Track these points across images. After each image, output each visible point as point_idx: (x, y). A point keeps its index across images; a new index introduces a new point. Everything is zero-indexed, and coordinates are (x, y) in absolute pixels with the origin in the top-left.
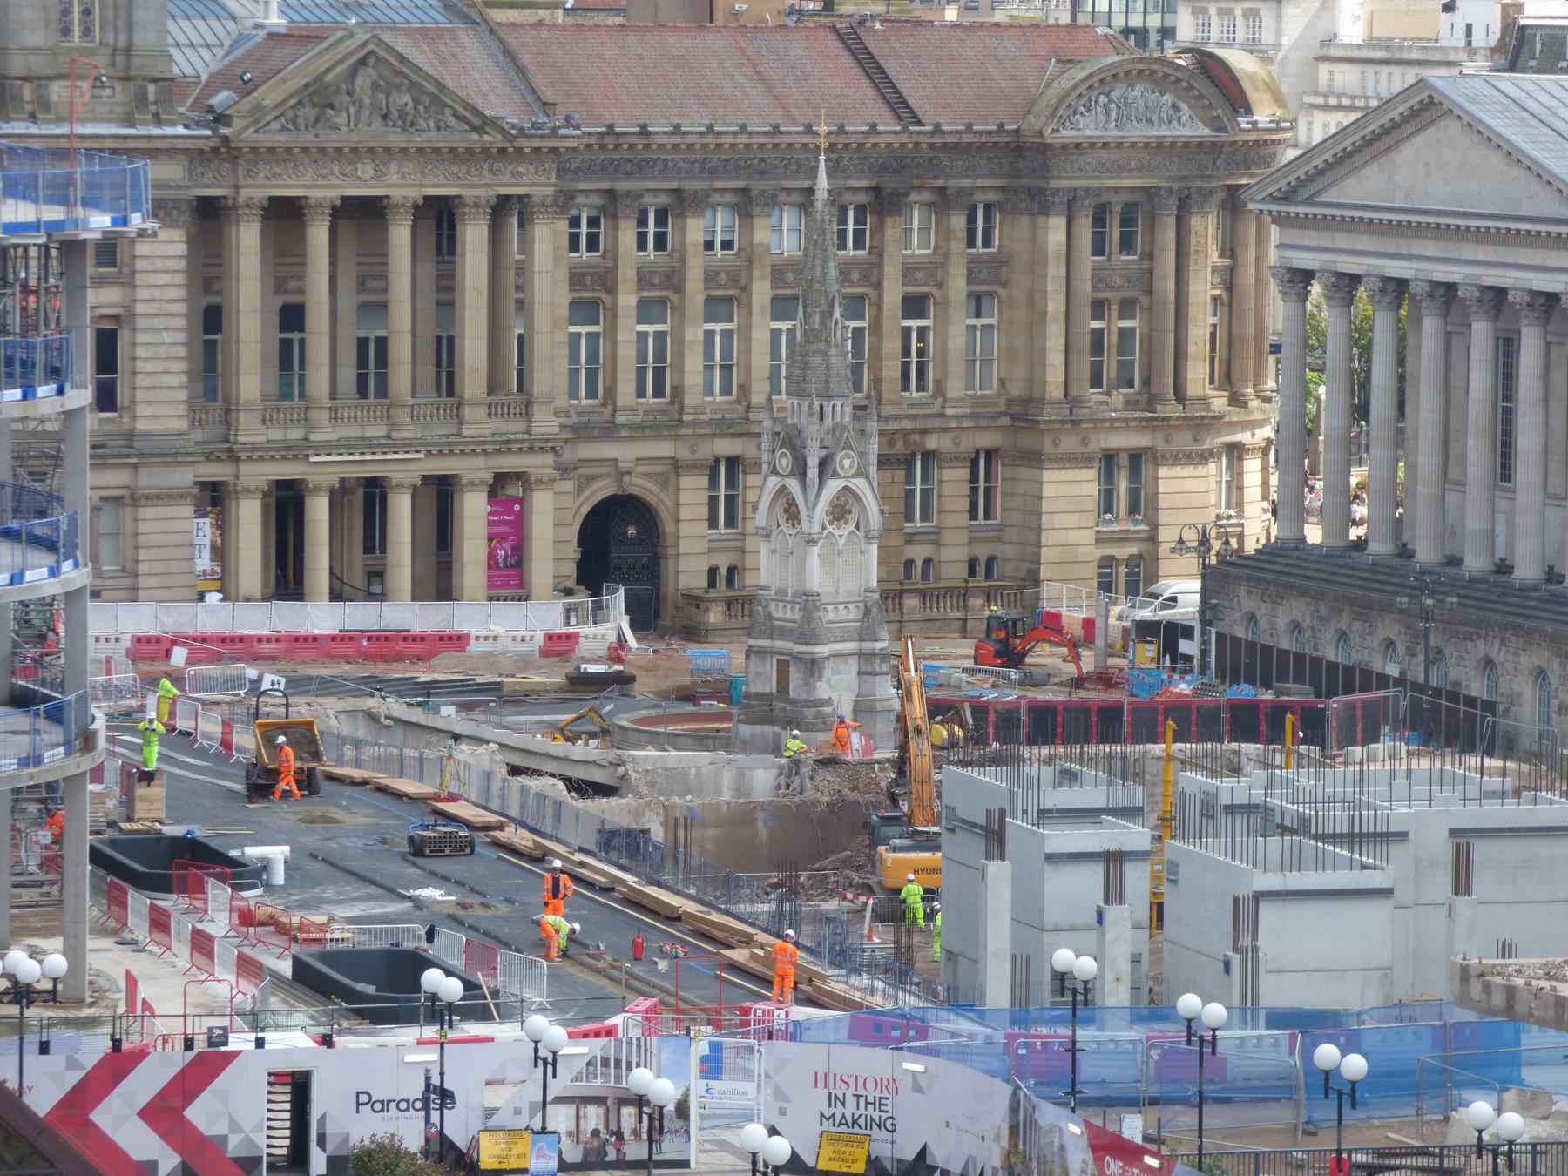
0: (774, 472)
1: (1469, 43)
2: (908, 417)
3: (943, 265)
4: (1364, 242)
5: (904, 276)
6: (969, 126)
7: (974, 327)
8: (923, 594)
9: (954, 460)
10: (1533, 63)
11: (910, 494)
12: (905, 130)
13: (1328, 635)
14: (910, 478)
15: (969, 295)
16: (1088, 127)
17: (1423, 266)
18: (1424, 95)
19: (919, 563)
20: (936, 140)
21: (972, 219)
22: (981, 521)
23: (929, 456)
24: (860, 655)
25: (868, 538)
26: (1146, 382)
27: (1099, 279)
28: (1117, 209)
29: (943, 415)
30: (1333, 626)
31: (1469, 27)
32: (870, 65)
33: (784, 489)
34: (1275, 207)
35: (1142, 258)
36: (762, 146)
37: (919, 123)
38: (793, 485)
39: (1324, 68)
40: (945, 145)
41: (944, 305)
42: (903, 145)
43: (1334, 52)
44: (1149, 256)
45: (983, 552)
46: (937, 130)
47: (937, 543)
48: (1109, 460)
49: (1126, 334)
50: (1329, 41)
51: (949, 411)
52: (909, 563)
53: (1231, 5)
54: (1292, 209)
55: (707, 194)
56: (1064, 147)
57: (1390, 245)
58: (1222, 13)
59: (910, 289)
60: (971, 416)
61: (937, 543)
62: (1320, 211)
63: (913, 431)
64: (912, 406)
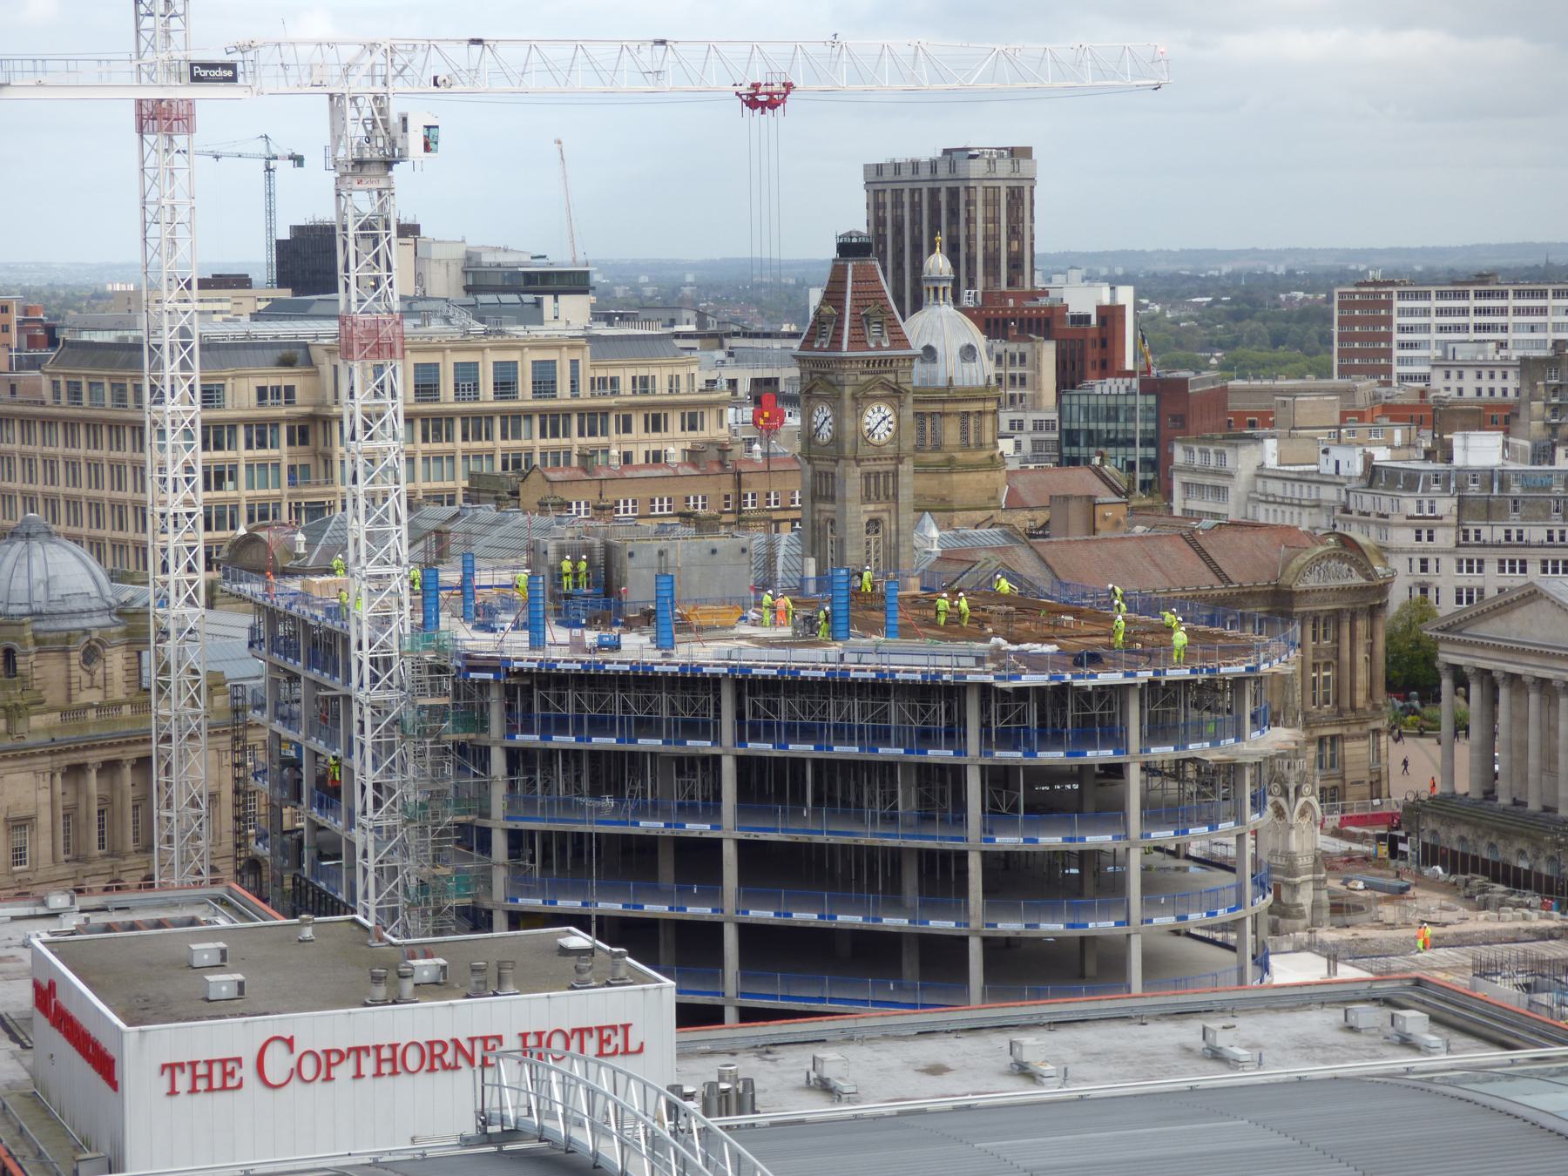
0: (1270, 794)
4: (1492, 654)
13: (1483, 845)
16: (1311, 582)
17: (1529, 669)
18: (1532, 589)
24: (1314, 880)
26: (1337, 701)
27: (1316, 651)
28: (1322, 620)
30: (1486, 840)
31: (1337, 463)
33: (1276, 802)
34: (1440, 635)
37: (1231, 583)
38: (1282, 801)
39: (1260, 482)
43: (1265, 473)
44: (1338, 641)
46: (1241, 586)
48: (1321, 740)
49: (1326, 679)
50: (1261, 466)
54: (1451, 636)
56: (1301, 592)
57: (1509, 657)
58: (1201, 451)
62: (1468, 639)
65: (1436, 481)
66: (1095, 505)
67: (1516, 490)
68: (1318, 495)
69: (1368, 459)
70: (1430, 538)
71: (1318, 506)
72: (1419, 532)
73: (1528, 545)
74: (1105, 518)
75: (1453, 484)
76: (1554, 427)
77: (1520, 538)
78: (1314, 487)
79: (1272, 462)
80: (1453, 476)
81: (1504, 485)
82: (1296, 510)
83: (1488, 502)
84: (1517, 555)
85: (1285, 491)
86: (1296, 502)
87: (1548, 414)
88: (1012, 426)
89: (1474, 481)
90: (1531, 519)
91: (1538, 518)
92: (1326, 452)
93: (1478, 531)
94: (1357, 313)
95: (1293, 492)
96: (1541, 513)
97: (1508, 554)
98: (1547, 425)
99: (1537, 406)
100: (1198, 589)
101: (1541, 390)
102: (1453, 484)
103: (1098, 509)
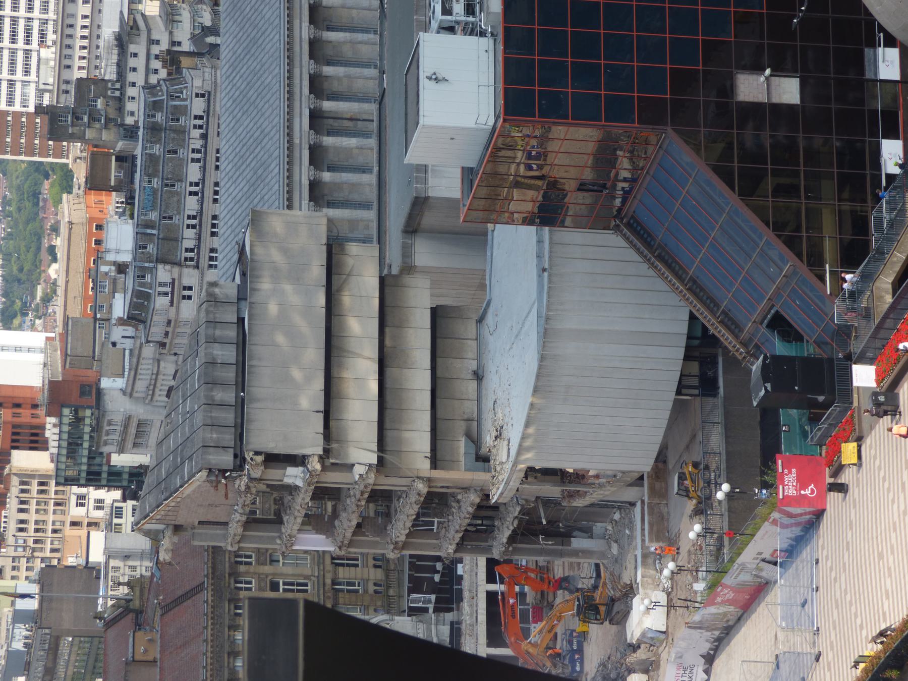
1: (133, 337)
2: (318, 590)
3: (259, 574)
5: (263, 590)
6: (205, 563)
7: (283, 563)
8: (389, 587)
9: (335, 573)
10: (143, 314)
11: (349, 591)
12: (207, 589)
14: (342, 590)
15: (270, 564)
19: (376, 588)
20: (210, 576)
21: (241, 563)
22: (359, 562)
23: (334, 583)
25: (393, 620)
29: (318, 577)
31: (123, 337)
32: (178, 601)
35: (258, 496)
36: (211, 647)
39: (135, 395)
40: (213, 573)
41: (274, 574)
42: (212, 590)
43: (129, 390)
45: (371, 562)
46: (207, 576)
47: (368, 580)
50: (124, 392)
51: (316, 574)
52: (376, 592)
53: (104, 431)
55: (230, 669)
58: (107, 434)
59: (268, 588)
60: (319, 566)
61: (368, 580)
63: (324, 589)
64: (314, 589)
65: (144, 277)
66: (133, 661)
67: (154, 216)
68: (149, 359)
69: (121, 322)
70: (190, 288)
71: (159, 361)
72: (184, 297)
73: (201, 212)
74: (146, 651)
75: (147, 265)
76: (108, 120)
77: (194, 217)
78: (142, 361)
79: (120, 383)
80: (139, 264)
81: (149, 225)
82: (161, 377)
83: (162, 239)
84: (207, 221)
85: (145, 379)
86: (154, 377)
87: (97, 125)
88: (83, 505)
89: (145, 247)
90: (179, 207)
91: (179, 201)
92: (114, 344)
93: (187, 250)
94: (8, 140)
95: (146, 374)
96: (175, 199)
97: (207, 229)
98: (106, 126)
99: (89, 134)
100: (206, 615)
101: (76, 130)
102: (147, 265)
103: (137, 658)
